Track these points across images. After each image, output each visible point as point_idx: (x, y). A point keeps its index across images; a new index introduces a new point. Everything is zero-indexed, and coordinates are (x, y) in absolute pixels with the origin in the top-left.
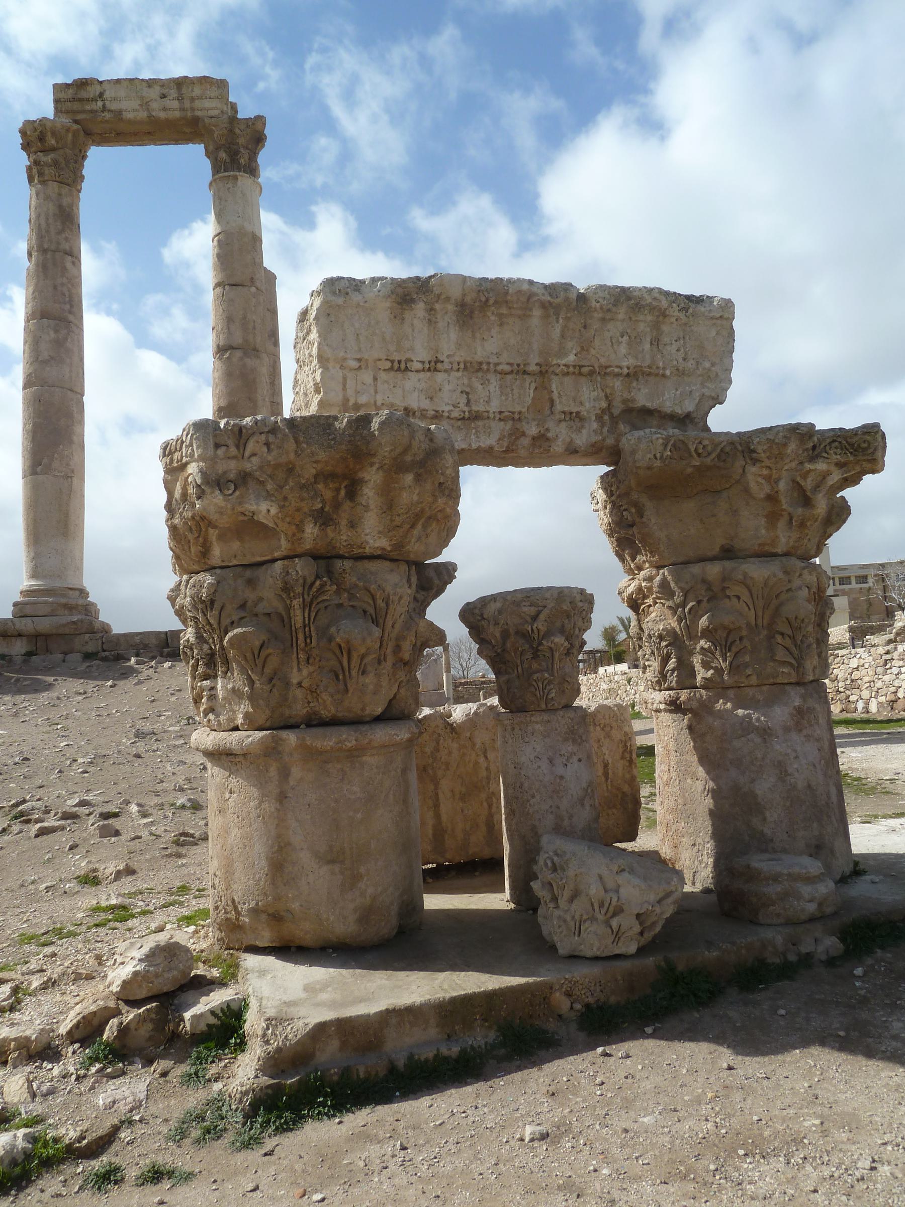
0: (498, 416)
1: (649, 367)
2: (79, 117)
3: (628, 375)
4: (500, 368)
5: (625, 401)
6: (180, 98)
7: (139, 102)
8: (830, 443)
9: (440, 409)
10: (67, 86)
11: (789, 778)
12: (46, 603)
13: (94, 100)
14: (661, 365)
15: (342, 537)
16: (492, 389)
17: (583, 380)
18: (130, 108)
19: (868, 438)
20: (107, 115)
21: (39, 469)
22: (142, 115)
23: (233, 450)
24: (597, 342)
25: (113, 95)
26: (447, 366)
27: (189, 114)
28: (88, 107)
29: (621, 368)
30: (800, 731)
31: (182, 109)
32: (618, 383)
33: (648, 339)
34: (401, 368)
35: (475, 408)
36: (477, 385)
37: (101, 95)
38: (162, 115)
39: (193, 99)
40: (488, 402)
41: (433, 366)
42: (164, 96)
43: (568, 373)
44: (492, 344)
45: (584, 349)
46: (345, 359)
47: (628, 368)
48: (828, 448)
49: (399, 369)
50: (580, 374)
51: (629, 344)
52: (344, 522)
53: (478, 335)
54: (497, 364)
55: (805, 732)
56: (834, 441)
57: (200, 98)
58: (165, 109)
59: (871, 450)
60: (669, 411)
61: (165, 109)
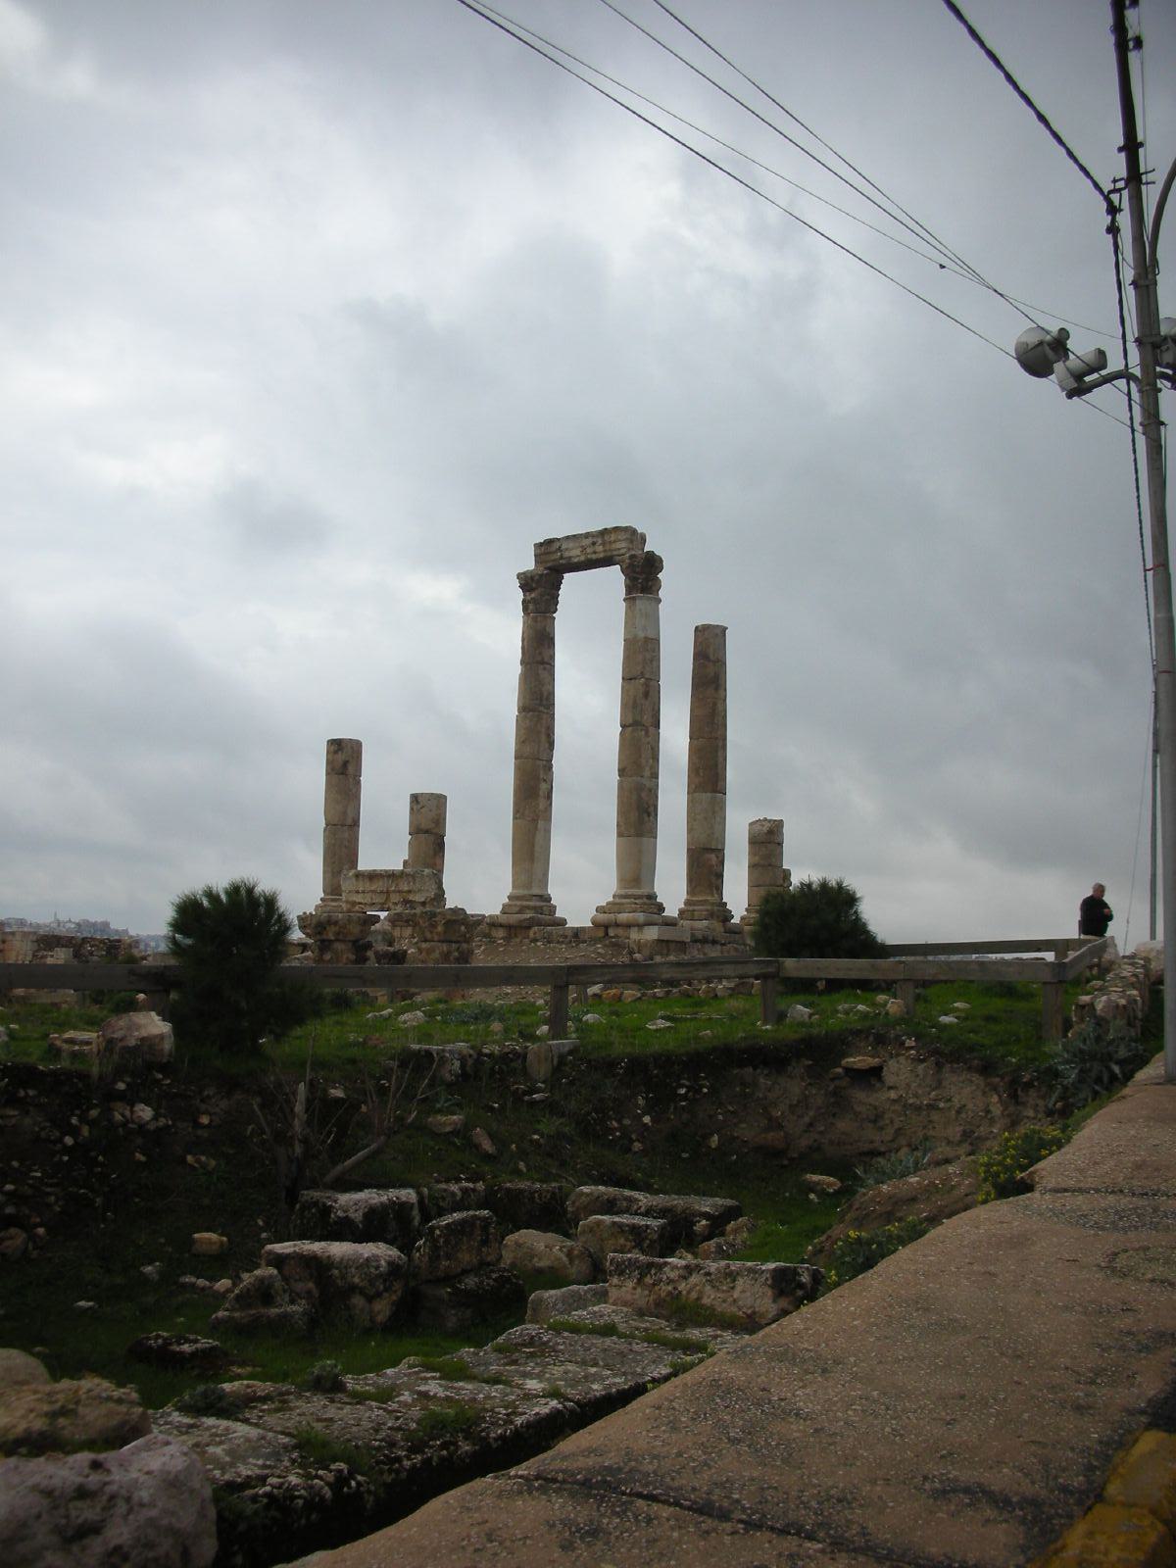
2: (549, 565)
6: (604, 544)
10: (541, 544)
12: (515, 905)
13: (556, 552)
15: (325, 937)
18: (575, 553)
21: (518, 816)
27: (609, 554)
28: (553, 558)
31: (605, 551)
34: (357, 892)
41: (363, 892)
44: (379, 885)
45: (397, 885)
57: (615, 542)
58: (595, 553)
61: (595, 553)
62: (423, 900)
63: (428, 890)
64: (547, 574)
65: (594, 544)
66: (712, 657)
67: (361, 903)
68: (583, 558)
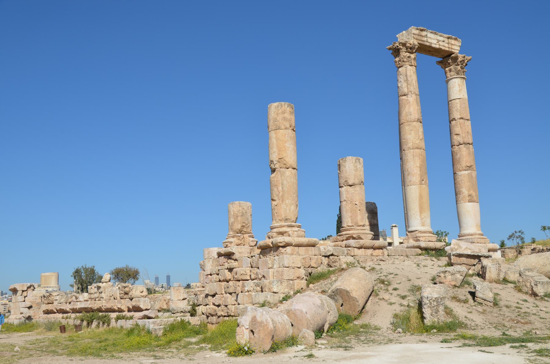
7: (437, 41)
20: (428, 44)
22: (437, 46)
27: (450, 50)
38: (443, 48)
39: (452, 45)
42: (443, 41)
58: (444, 46)
61: (444, 46)
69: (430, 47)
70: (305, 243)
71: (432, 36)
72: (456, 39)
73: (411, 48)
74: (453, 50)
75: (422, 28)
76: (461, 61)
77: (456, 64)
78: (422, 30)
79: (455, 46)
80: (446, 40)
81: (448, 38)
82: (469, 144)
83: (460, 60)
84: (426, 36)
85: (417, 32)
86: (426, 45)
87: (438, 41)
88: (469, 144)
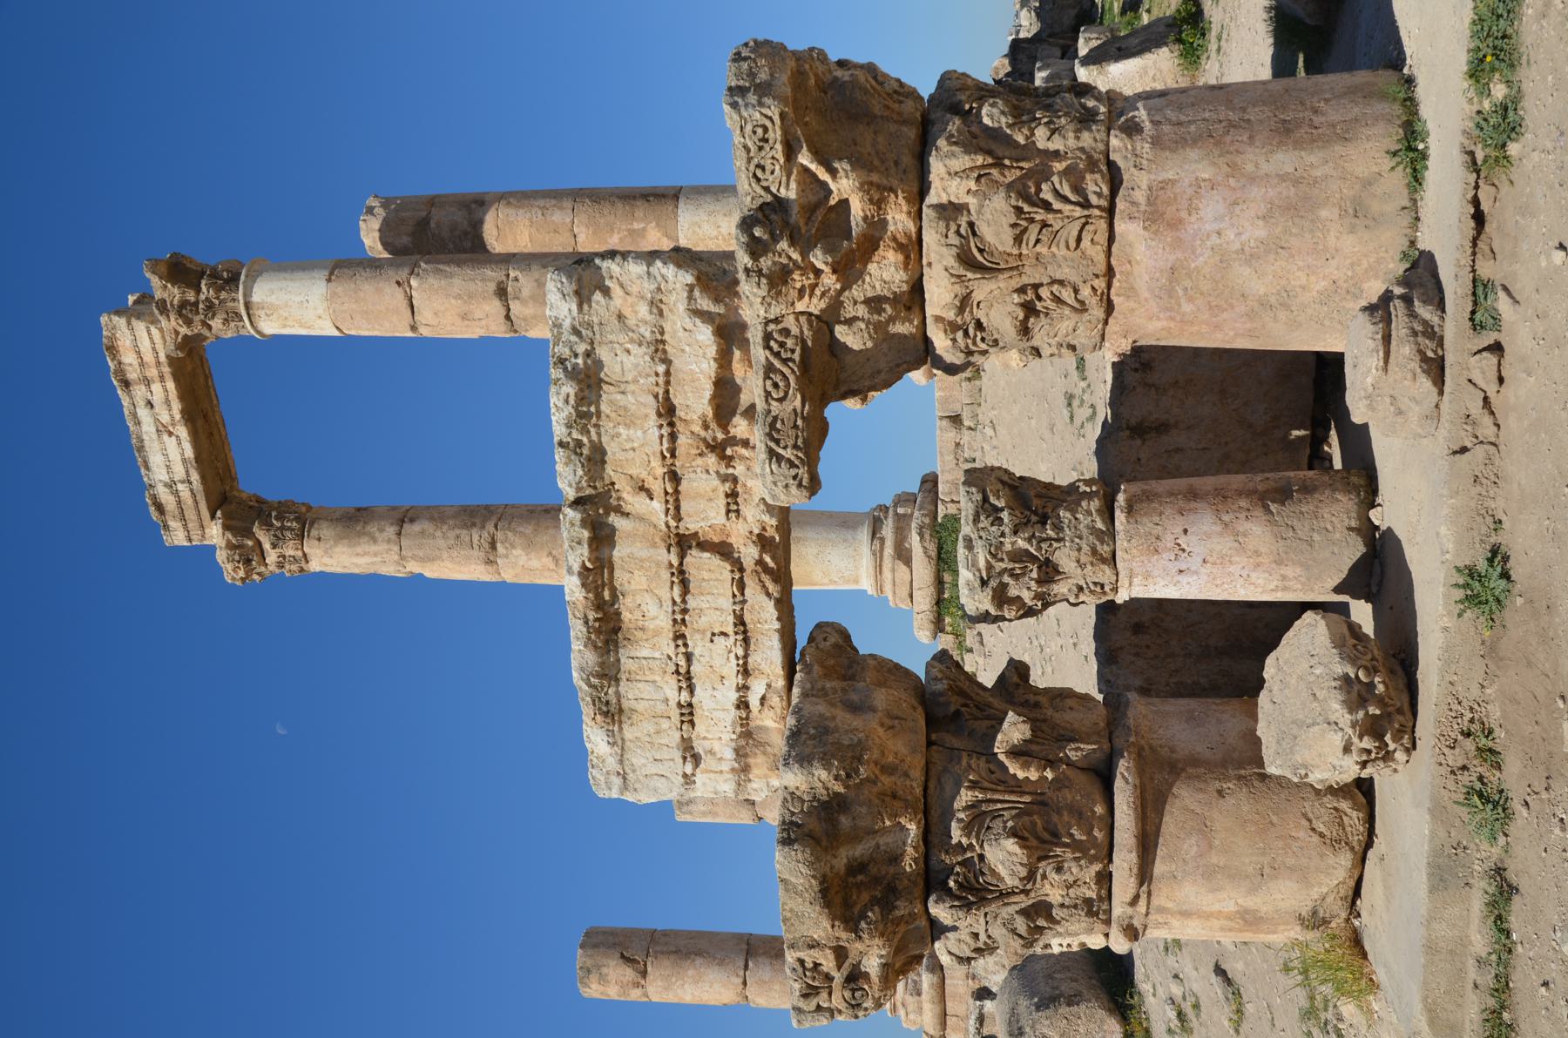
0: (739, 598)
1: (656, 397)
2: (205, 513)
3: (671, 424)
4: (678, 600)
5: (706, 427)
6: (147, 382)
7: (165, 437)
8: (758, 180)
9: (735, 669)
11: (1247, 249)
12: (893, 571)
13: (176, 493)
14: (653, 379)
16: (704, 606)
17: (683, 487)
19: (749, 128)
20: (195, 477)
23: (824, 995)
24: (634, 472)
25: (164, 471)
26: (682, 663)
27: (166, 370)
28: (190, 502)
29: (662, 436)
30: (1181, 221)
32: (683, 440)
33: (619, 397)
34: (688, 713)
35: (730, 629)
36: (703, 622)
37: (166, 485)
38: (176, 406)
39: (142, 364)
40: (722, 610)
42: (150, 404)
43: (678, 508)
46: (685, 776)
47: (661, 426)
48: (765, 184)
49: (691, 714)
50: (677, 492)
51: (627, 426)
52: (892, 870)
53: (640, 623)
54: (674, 603)
55: (1184, 214)
56: (755, 175)
57: (139, 353)
59: (768, 124)
60: (714, 365)
61: (167, 402)
62: (705, 335)
63: (657, 306)
64: (226, 516)
65: (150, 404)
66: (424, 214)
67: (743, 704)
68: (183, 432)
69: (198, 459)
70: (938, 1009)
71: (156, 460)
72: (113, 349)
73: (248, 561)
74: (163, 358)
75: (152, 509)
76: (189, 322)
77: (205, 332)
78: (160, 508)
79: (141, 344)
80: (139, 391)
81: (126, 384)
82: (508, 317)
83: (184, 330)
84: (170, 485)
85: (174, 524)
86: (203, 478)
87: (163, 430)
88: (508, 317)
